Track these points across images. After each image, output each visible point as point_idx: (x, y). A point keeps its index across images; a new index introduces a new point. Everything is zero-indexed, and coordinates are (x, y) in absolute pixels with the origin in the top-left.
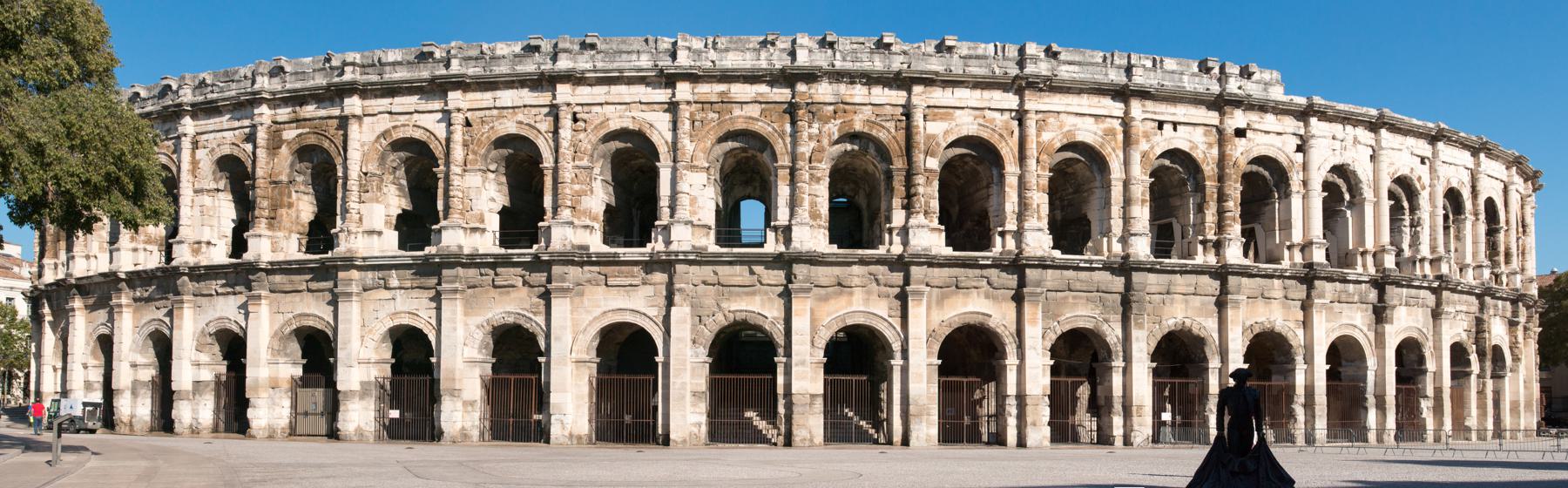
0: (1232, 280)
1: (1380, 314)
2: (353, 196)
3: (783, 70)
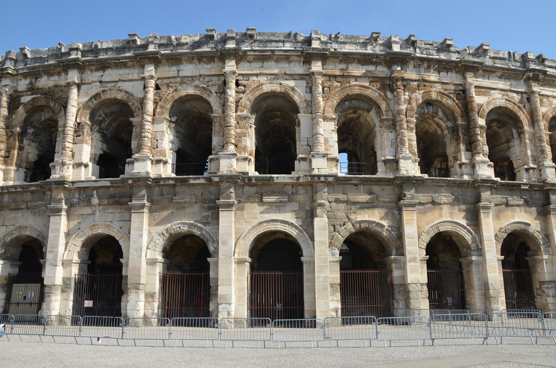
2: (70, 138)
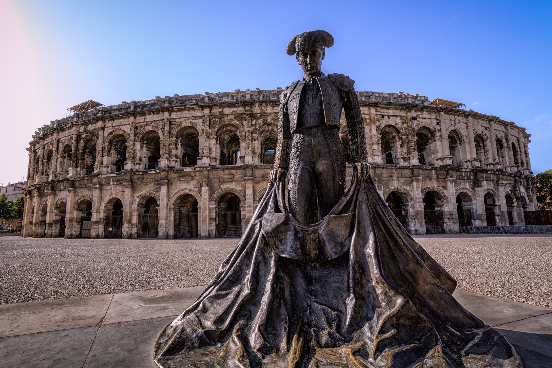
1: (476, 183)
3: (241, 102)
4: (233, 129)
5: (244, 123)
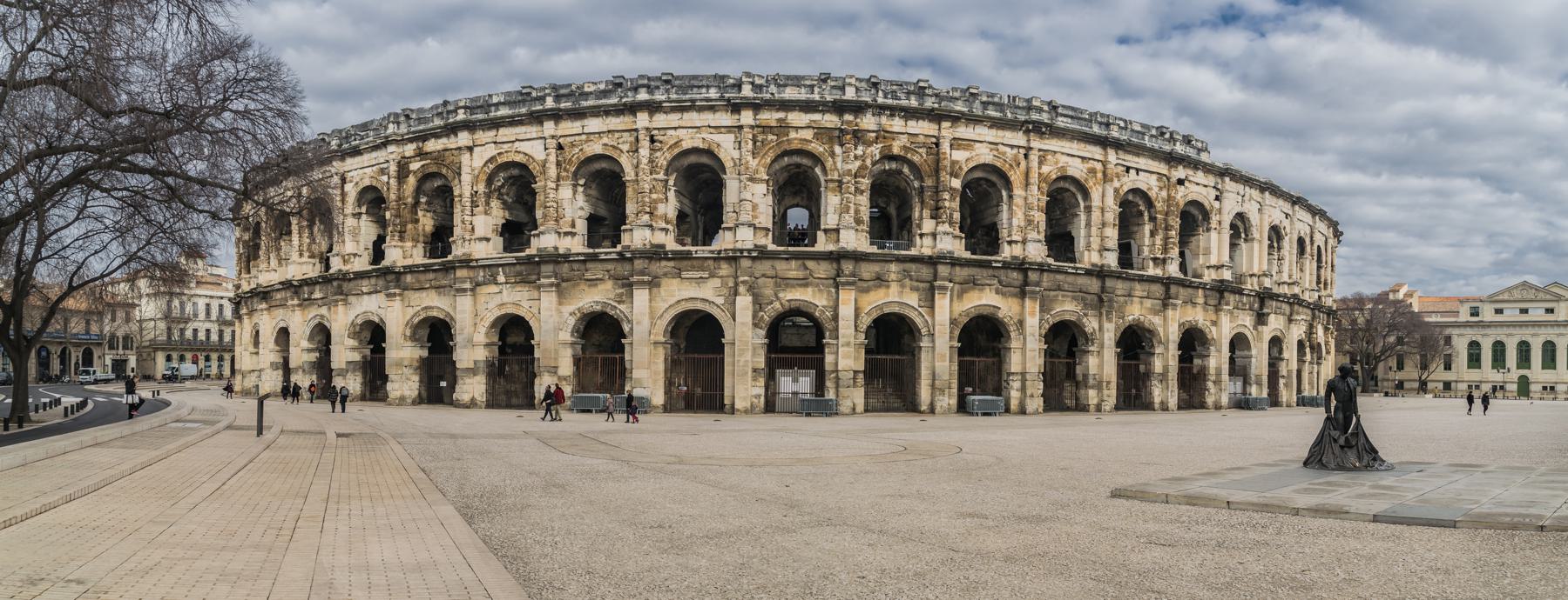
0: (1173, 289)
1: (1261, 319)
3: (835, 102)
4: (805, 161)
5: (838, 150)
